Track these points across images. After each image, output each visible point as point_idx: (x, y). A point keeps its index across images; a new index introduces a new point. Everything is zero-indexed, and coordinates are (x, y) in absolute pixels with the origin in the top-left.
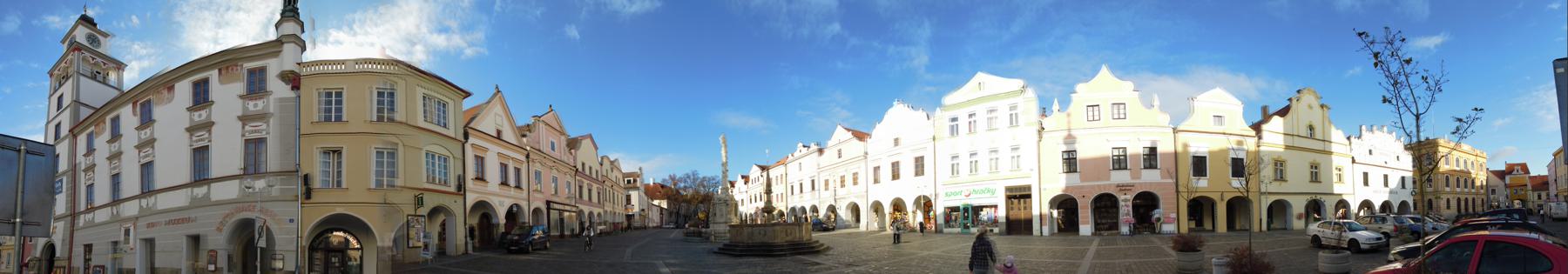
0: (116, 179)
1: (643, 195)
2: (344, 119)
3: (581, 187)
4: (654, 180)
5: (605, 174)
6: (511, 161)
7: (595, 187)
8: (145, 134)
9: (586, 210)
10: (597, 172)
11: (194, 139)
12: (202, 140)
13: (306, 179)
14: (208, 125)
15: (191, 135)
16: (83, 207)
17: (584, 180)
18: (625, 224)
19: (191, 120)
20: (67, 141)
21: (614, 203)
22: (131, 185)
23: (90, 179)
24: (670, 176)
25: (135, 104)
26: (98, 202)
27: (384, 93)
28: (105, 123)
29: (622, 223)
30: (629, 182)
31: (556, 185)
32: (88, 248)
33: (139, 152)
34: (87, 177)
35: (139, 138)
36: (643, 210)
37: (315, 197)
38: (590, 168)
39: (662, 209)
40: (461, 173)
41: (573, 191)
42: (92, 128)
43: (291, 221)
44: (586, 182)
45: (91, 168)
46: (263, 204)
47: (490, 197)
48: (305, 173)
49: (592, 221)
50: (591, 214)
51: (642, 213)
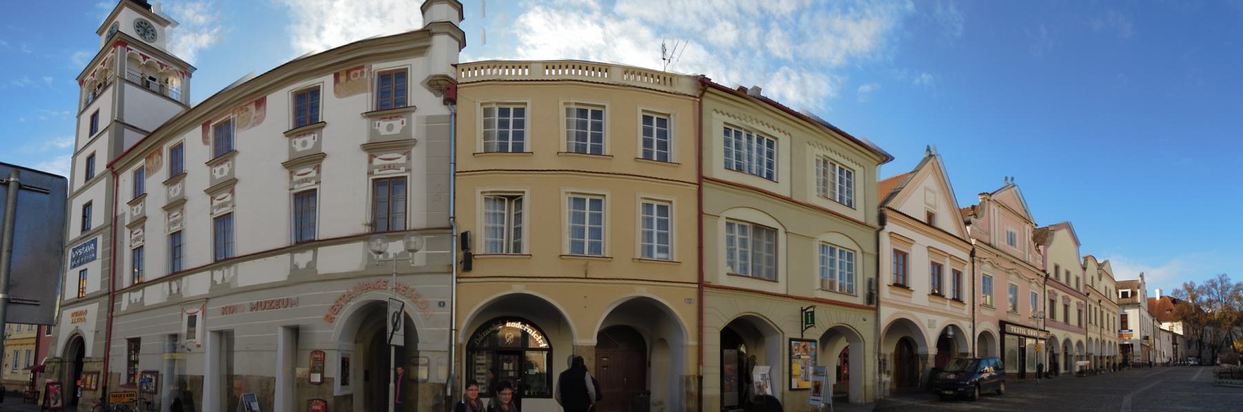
0: (176, 239)
1: (1146, 314)
2: (527, 148)
3: (1052, 302)
4: (1161, 292)
5: (1089, 283)
6: (948, 260)
7: (1074, 302)
8: (221, 172)
9: (1060, 336)
10: (1078, 279)
11: (296, 178)
12: (306, 181)
13: (465, 240)
14: (316, 159)
15: (291, 173)
16: (126, 283)
17: (1057, 291)
18: (1119, 359)
19: (291, 150)
20: (103, 183)
21: (1102, 327)
22: (198, 249)
23: (137, 239)
24: (1185, 285)
25: (205, 127)
26: (150, 272)
27: (587, 110)
28: (161, 154)
29: (1114, 357)
30: (1125, 295)
31: (1016, 297)
32: (134, 344)
33: (212, 199)
34: (133, 237)
35: (212, 177)
36: (1147, 338)
37: (478, 268)
38: (1068, 273)
39: (1175, 336)
40: (873, 276)
41: (1040, 309)
42: (142, 162)
43: (442, 304)
44: (1060, 294)
45: (140, 222)
46: (401, 280)
47: (914, 313)
48: (463, 231)
49: (1069, 353)
50: (1067, 342)
51: (1145, 342)
